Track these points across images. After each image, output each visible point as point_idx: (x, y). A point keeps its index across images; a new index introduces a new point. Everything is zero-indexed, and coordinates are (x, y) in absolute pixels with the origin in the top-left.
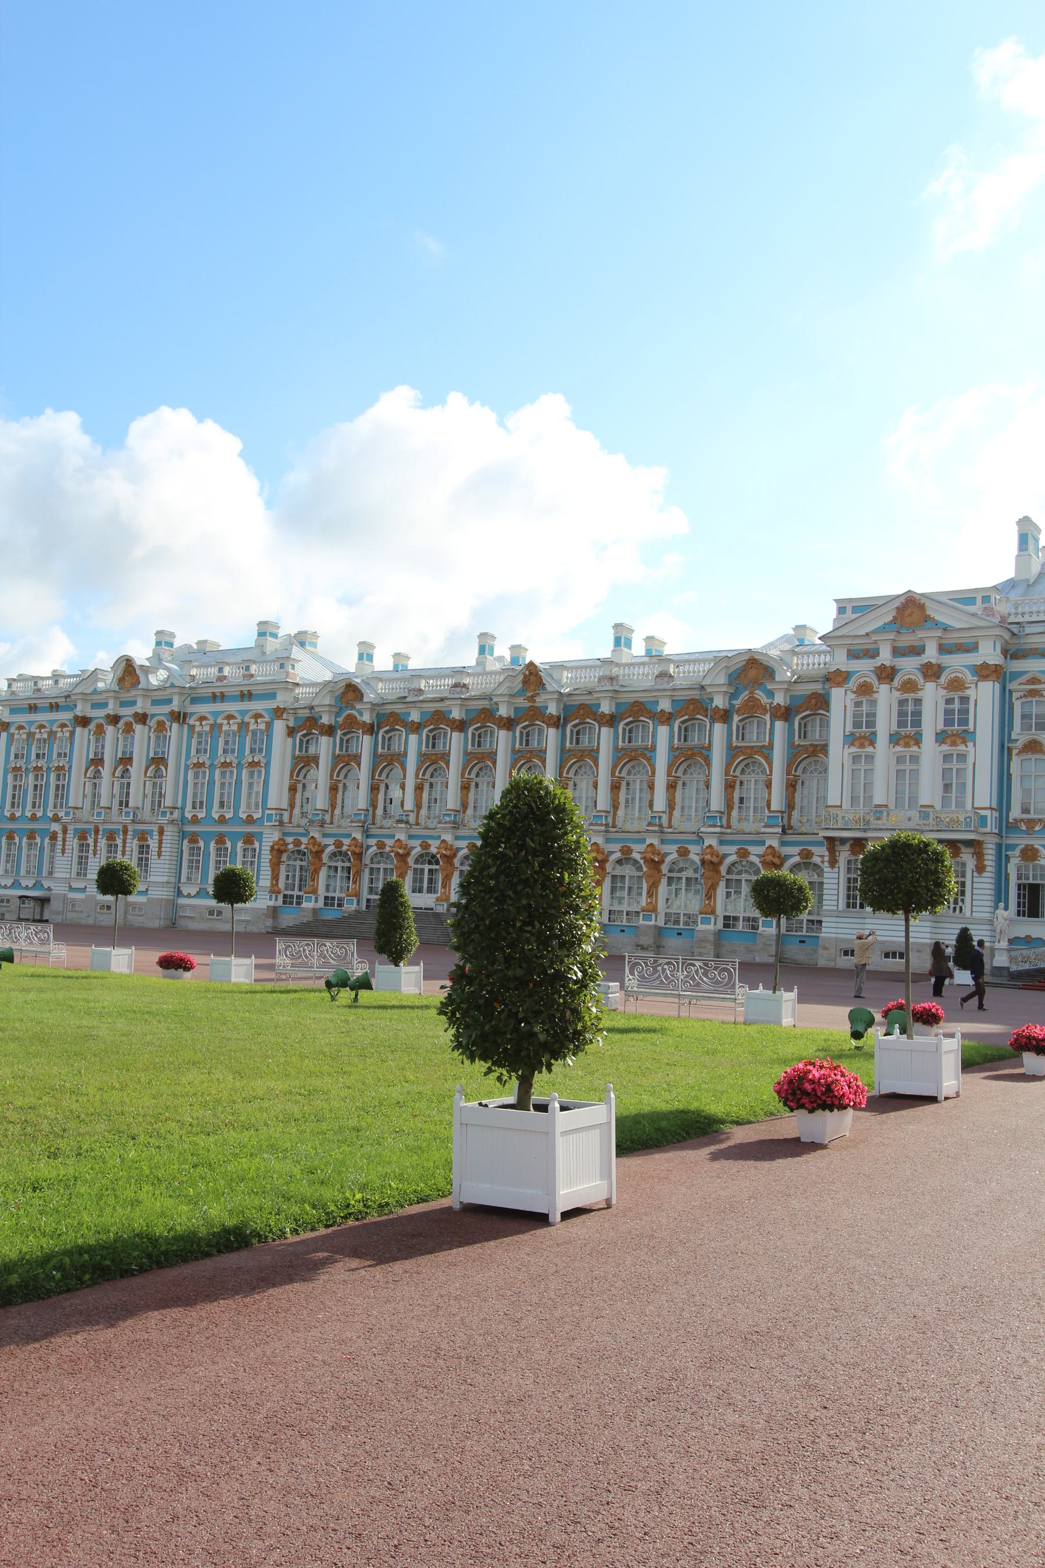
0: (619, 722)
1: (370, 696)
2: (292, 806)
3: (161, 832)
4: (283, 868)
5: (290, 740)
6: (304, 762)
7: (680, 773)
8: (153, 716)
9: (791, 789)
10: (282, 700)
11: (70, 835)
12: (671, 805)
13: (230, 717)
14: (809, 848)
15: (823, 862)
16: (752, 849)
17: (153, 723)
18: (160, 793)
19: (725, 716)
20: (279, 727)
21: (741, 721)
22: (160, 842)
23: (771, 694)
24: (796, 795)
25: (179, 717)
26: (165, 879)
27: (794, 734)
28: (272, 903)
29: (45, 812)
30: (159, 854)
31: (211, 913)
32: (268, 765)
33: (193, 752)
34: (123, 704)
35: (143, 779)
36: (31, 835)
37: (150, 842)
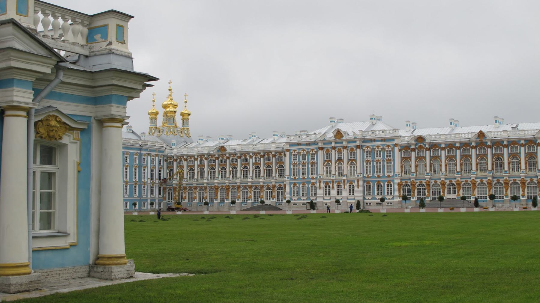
2: (402, 172)
3: (358, 181)
4: (401, 190)
6: (405, 159)
8: (349, 147)
10: (396, 141)
11: (322, 183)
13: (378, 147)
17: (349, 149)
18: (354, 170)
20: (396, 149)
22: (358, 184)
25: (359, 147)
26: (361, 195)
29: (308, 176)
30: (358, 188)
31: (377, 204)
32: (394, 160)
33: (365, 157)
34: (336, 143)
36: (304, 184)
37: (354, 184)
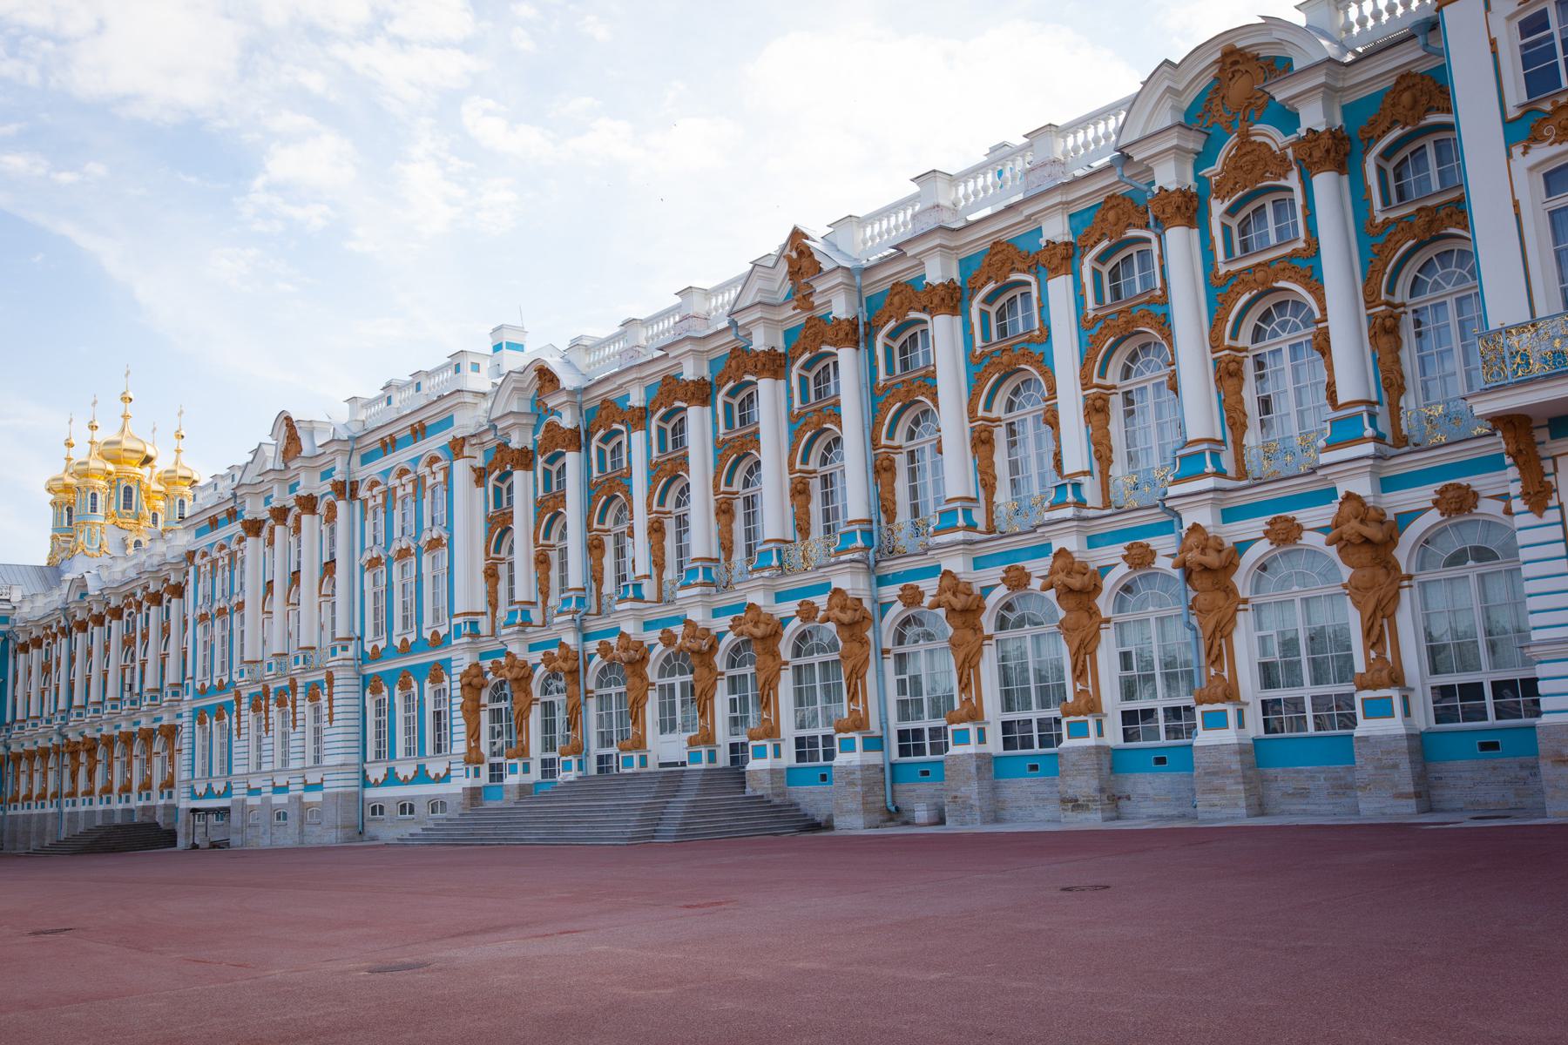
0: (971, 298)
1: (568, 380)
2: (493, 603)
5: (480, 491)
7: (1113, 376)
9: (1384, 340)
12: (1102, 453)
14: (1463, 481)
15: (1508, 512)
16: (1305, 516)
19: (1188, 208)
20: (461, 470)
21: (1231, 212)
23: (1288, 118)
24: (1405, 355)
27: (1369, 199)
28: (469, 782)
35: (317, 600)
